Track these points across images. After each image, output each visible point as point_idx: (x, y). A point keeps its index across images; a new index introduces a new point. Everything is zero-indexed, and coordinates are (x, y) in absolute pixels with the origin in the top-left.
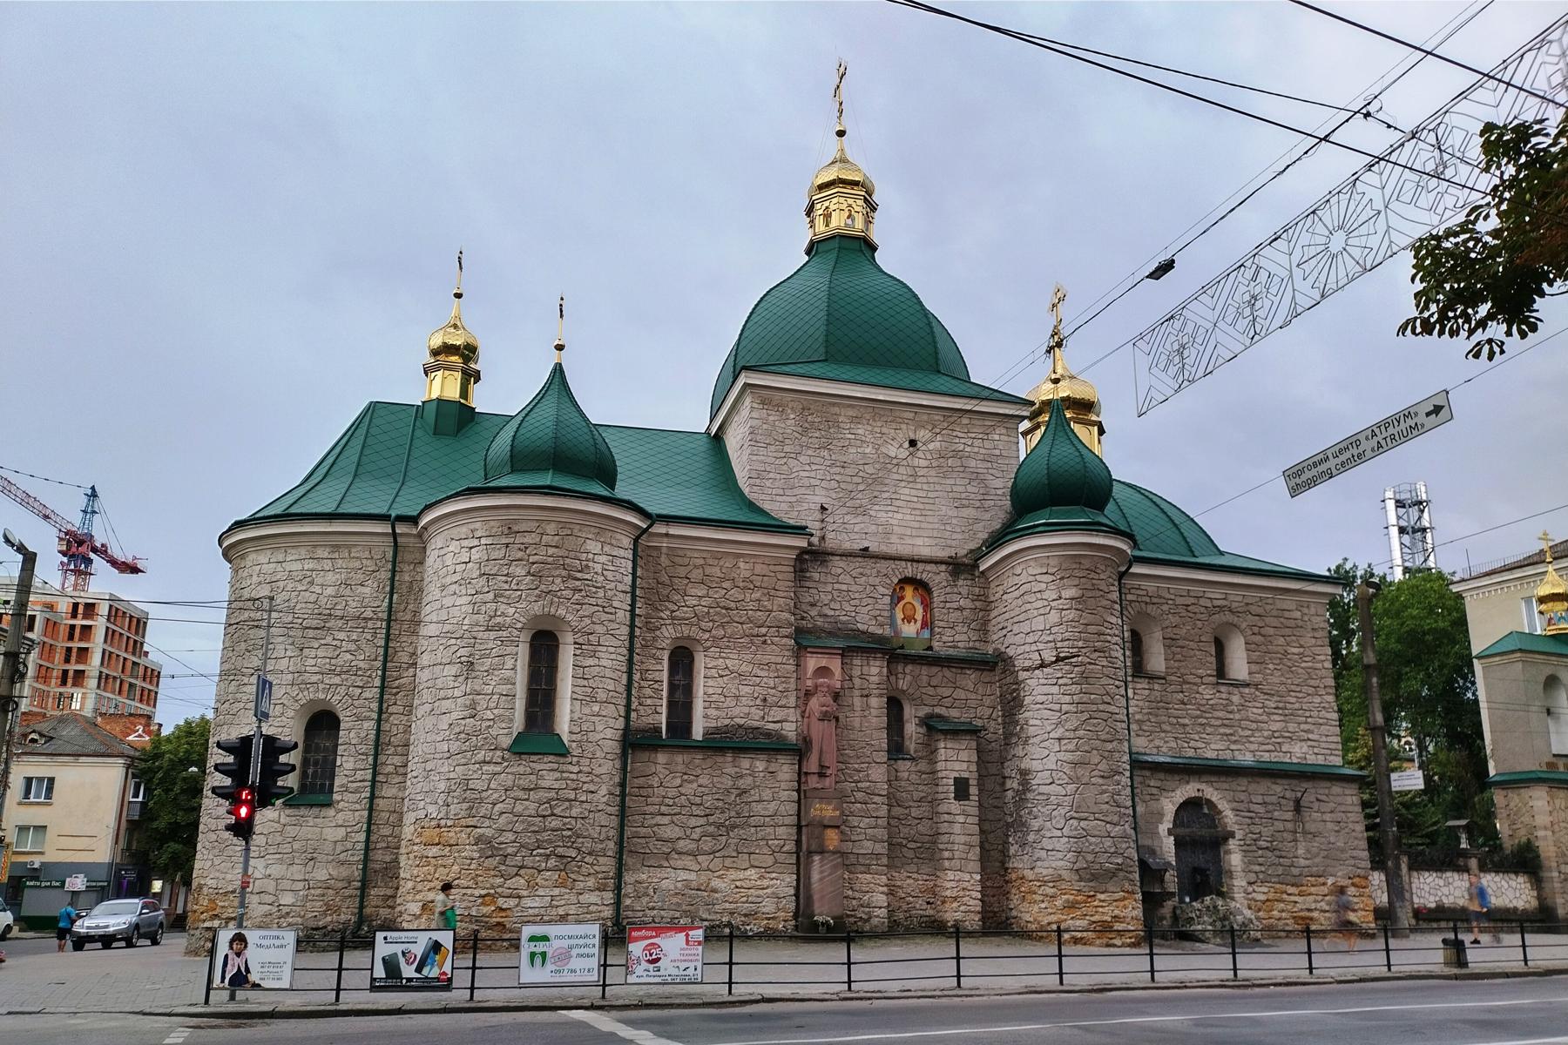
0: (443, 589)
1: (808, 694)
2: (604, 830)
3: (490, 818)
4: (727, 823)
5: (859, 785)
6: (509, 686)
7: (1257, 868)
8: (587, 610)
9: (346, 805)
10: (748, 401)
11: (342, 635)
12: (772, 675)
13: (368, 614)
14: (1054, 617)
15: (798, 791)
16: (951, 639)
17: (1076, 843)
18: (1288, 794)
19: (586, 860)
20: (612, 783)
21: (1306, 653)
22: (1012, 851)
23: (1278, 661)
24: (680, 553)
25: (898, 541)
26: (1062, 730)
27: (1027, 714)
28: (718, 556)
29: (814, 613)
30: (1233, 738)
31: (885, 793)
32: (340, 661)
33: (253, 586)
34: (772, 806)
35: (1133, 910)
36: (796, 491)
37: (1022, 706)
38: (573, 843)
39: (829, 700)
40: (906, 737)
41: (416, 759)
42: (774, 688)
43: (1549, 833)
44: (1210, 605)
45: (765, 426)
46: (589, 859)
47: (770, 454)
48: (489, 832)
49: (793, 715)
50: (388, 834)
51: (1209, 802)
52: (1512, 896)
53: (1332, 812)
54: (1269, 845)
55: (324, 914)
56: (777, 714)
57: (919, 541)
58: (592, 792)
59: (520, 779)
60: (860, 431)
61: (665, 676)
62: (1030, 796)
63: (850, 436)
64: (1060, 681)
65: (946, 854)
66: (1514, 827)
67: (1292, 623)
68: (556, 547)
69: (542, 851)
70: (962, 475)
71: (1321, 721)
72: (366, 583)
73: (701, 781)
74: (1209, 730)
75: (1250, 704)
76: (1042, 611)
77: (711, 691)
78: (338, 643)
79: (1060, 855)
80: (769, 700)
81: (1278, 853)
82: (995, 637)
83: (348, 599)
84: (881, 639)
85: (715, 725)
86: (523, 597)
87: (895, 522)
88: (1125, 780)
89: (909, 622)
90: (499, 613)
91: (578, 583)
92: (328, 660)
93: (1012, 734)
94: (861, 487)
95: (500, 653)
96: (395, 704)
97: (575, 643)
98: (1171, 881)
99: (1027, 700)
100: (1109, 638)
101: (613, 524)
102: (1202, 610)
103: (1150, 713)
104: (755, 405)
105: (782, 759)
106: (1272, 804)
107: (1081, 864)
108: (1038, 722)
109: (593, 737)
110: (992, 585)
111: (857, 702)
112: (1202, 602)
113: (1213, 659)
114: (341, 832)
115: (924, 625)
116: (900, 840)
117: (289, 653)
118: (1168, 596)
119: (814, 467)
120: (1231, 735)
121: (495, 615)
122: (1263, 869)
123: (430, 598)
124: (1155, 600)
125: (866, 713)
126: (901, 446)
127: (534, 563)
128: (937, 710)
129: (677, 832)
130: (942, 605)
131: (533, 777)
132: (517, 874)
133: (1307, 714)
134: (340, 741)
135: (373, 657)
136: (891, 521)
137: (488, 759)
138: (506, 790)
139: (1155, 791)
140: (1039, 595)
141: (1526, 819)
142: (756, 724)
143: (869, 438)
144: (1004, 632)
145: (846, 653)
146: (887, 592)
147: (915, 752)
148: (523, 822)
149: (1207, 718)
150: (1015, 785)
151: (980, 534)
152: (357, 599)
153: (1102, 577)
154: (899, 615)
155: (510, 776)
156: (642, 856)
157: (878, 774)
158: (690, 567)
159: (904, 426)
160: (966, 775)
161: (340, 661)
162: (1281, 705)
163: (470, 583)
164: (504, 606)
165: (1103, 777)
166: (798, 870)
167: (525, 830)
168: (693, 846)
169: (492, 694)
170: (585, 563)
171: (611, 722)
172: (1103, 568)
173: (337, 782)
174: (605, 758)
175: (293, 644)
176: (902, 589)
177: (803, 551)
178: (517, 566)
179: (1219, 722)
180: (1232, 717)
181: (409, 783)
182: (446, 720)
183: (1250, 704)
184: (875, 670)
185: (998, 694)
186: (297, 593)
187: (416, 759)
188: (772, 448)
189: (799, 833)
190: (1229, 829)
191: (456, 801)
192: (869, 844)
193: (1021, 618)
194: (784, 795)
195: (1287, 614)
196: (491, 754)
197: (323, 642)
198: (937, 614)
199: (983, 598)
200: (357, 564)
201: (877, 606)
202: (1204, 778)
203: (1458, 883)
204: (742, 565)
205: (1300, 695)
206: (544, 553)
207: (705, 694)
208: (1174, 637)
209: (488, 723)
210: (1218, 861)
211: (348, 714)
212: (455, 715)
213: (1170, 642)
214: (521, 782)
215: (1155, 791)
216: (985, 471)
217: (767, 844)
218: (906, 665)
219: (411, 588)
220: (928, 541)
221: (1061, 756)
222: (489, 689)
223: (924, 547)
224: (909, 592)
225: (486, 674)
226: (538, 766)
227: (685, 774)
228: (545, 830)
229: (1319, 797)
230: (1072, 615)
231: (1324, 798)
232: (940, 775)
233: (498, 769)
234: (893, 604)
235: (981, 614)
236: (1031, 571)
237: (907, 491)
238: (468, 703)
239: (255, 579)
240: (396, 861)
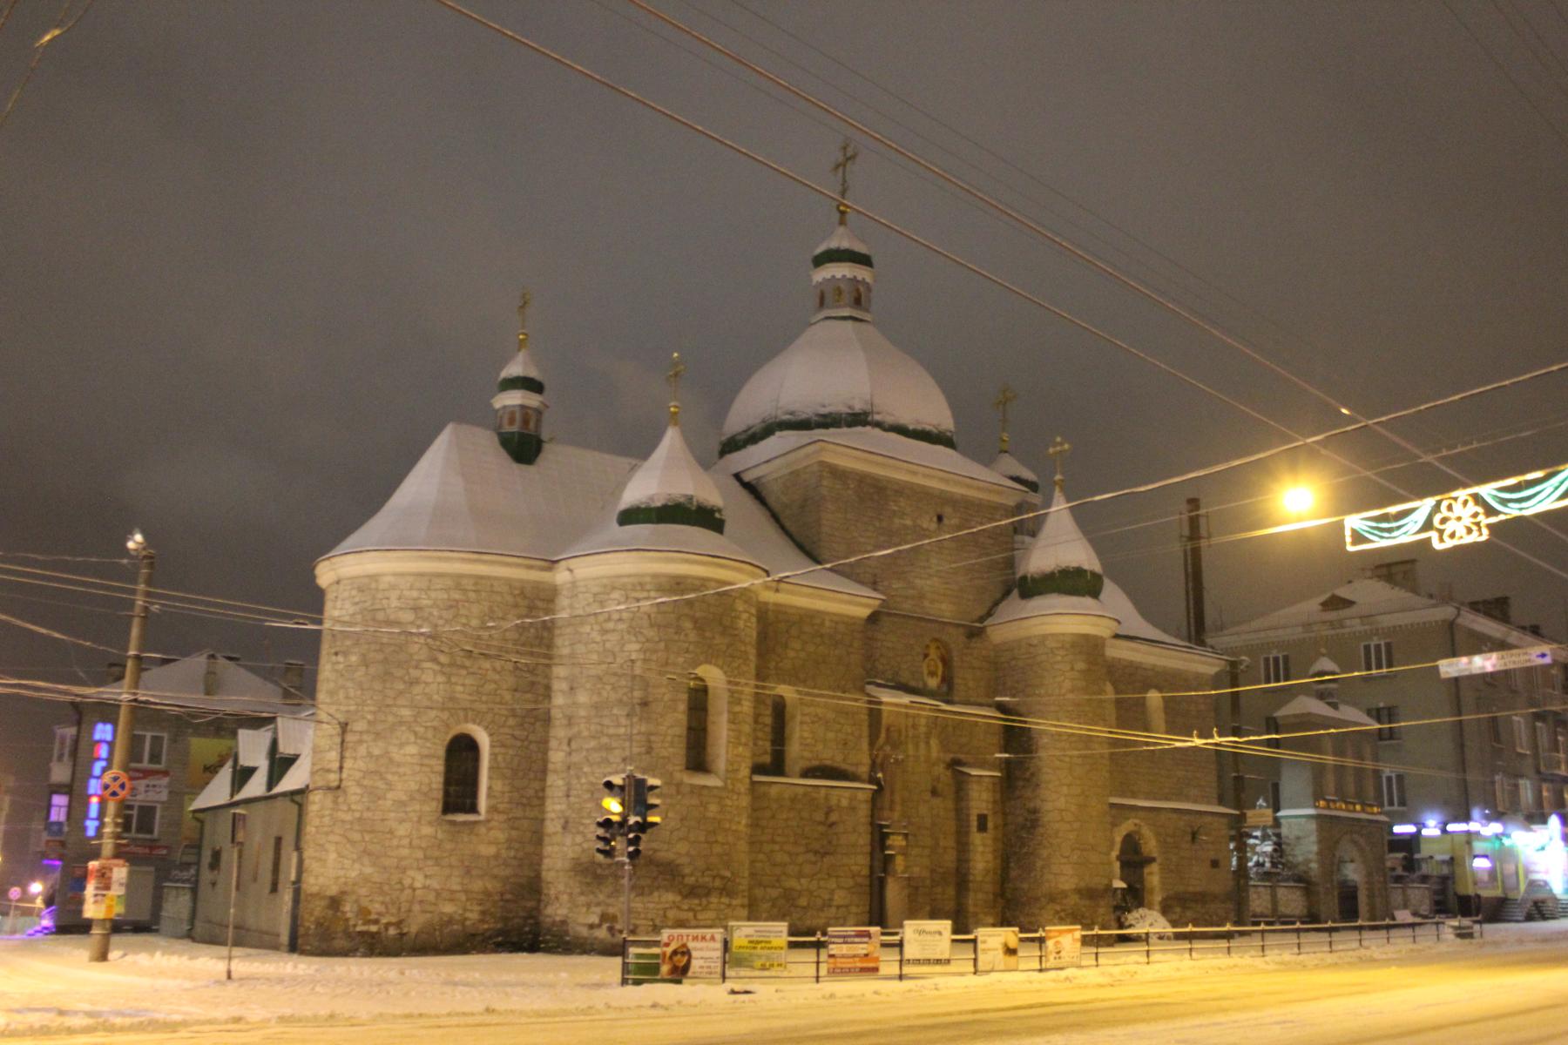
0: (604, 632)
15: (872, 824)
22: (1013, 874)
55: (482, 921)
60: (902, 504)
69: (709, 872)
115: (944, 680)
126: (931, 519)
129: (786, 859)
131: (702, 809)
142: (836, 765)
154: (925, 672)
160: (985, 812)
189: (872, 859)
197: (471, 670)
239: (394, 603)
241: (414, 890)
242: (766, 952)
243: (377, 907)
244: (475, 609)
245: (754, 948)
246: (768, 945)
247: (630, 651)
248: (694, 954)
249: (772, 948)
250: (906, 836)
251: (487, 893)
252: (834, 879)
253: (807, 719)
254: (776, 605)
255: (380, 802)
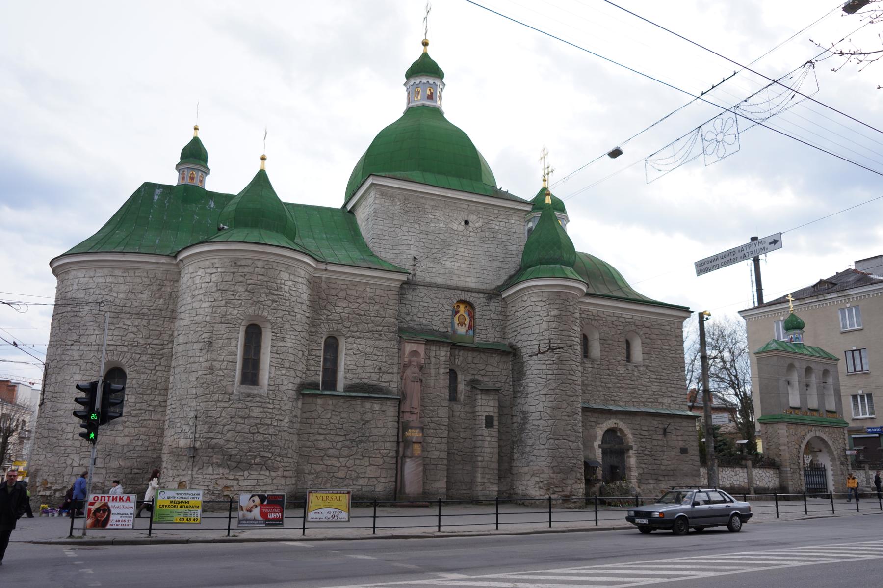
0: (193, 296)
1: (406, 366)
2: (287, 442)
3: (222, 433)
4: (357, 440)
5: (432, 419)
6: (234, 357)
7: (643, 466)
8: (280, 313)
9: (130, 424)
10: (373, 193)
11: (129, 323)
12: (384, 354)
13: (145, 311)
14: (545, 326)
15: (398, 422)
16: (485, 337)
17: (552, 452)
18: (661, 426)
19: (277, 459)
20: (291, 415)
21: (672, 349)
22: (516, 456)
23: (658, 353)
24: (333, 281)
25: (457, 279)
26: (547, 390)
27: (528, 380)
28: (355, 284)
29: (408, 318)
30: (634, 395)
31: (446, 424)
32: (127, 338)
33: (74, 291)
34: (383, 431)
35: (581, 488)
36: (400, 247)
37: (525, 376)
38: (270, 449)
39: (417, 370)
40: (458, 392)
41: (175, 398)
42: (385, 362)
43: (786, 447)
44: (624, 321)
45: (383, 209)
46: (278, 459)
47: (386, 225)
48: (221, 442)
49: (396, 378)
50: (155, 441)
51: (621, 431)
52: (767, 481)
53: (682, 435)
54: (649, 453)
56: (386, 377)
57: (469, 279)
58: (281, 420)
59: (239, 411)
60: (437, 214)
61: (322, 352)
62: (528, 426)
63: (431, 217)
64: (547, 362)
65: (480, 459)
66: (770, 444)
67: (665, 333)
68: (263, 275)
70: (493, 242)
71: (678, 386)
72: (144, 292)
73: (342, 415)
74: (622, 390)
75: (643, 377)
76: (538, 322)
77: (349, 363)
78: (126, 327)
79: (543, 459)
80: (383, 369)
81: (654, 457)
82: (510, 336)
83: (133, 301)
84: (445, 335)
85: (350, 383)
86: (243, 304)
87: (455, 268)
88: (580, 418)
89: (462, 326)
90: (228, 313)
91: (275, 297)
92: (120, 337)
93: (518, 391)
94: (437, 247)
95: (228, 337)
96: (160, 364)
97: (273, 332)
98: (599, 472)
99: (528, 372)
100: (574, 338)
101: (296, 262)
102: (621, 324)
103: (592, 381)
104: (377, 196)
105: (389, 403)
106: (652, 431)
107: (555, 464)
108: (533, 385)
109: (283, 388)
110: (509, 306)
111: (433, 371)
112: (621, 320)
113: (625, 351)
114: (127, 440)
115: (470, 328)
116: (454, 451)
117: (96, 332)
118: (603, 315)
119: (410, 234)
120: (633, 393)
121: (226, 314)
122: (646, 466)
123: (184, 302)
124: (596, 318)
125: (438, 378)
127: (249, 284)
128: (476, 377)
129: (328, 445)
130: (481, 317)
131: (247, 411)
132: (236, 467)
133: (672, 382)
134: (127, 386)
135: (147, 336)
136: (453, 267)
137: (220, 399)
138: (231, 417)
139: (593, 424)
140: (537, 313)
141: (775, 440)
142: (375, 383)
143: (442, 218)
144: (516, 333)
145: (428, 342)
146: (449, 308)
147: (464, 400)
148: (241, 436)
149: (620, 384)
150: (519, 420)
151: (503, 276)
152: (138, 301)
153: (571, 304)
154: (457, 322)
155: (233, 410)
156: (307, 458)
157: (443, 413)
158: (338, 290)
159: (462, 213)
160: (492, 414)
161: (127, 338)
162: (658, 377)
163: (210, 295)
164: (231, 309)
165: (568, 416)
166: (397, 467)
167: (242, 441)
168: (337, 452)
169: (223, 361)
170: (279, 285)
171: (292, 380)
172: (571, 299)
173: (125, 410)
174: (288, 400)
175: (99, 327)
176: (458, 306)
177: (404, 283)
178: (239, 286)
179: (627, 386)
180: (633, 383)
181: (168, 412)
182: (194, 375)
183: (643, 377)
184: (443, 353)
185: (511, 368)
186: (102, 296)
187: (175, 398)
188: (387, 222)
190: (630, 444)
191: (201, 423)
192: (437, 453)
193: (526, 326)
194: (390, 425)
195: (663, 327)
196: (222, 396)
197: (117, 326)
198: (477, 322)
199: (503, 313)
200: (139, 280)
201: (444, 316)
202: (620, 416)
203: (741, 474)
204: (368, 289)
205: (668, 372)
206: (256, 279)
207: (345, 364)
208: (605, 338)
209: (221, 378)
210: (623, 462)
211: (132, 369)
212: (200, 373)
213: (603, 340)
214: (240, 413)
215: (593, 424)
216: (506, 241)
217: (380, 452)
218: (460, 350)
219: (170, 296)
220: (476, 280)
221: (546, 404)
222: (221, 358)
223: (471, 282)
224: (462, 308)
225: (219, 349)
226: (249, 404)
227: (334, 411)
228: (254, 442)
229: (676, 427)
230: (554, 325)
231: (679, 428)
232: (477, 414)
233: (226, 405)
234: (454, 315)
235: (502, 323)
236: (532, 299)
237: (462, 250)
238: (208, 365)
239: (75, 286)
240: (159, 458)
241: (73, 467)
242: (183, 510)
243: (50, 479)
244: (123, 288)
245: (175, 507)
246: (186, 505)
247: (204, 308)
248: (113, 511)
249: (190, 506)
250: (422, 429)
251: (120, 469)
252: (367, 459)
253: (351, 352)
254: (327, 278)
255: (59, 411)
